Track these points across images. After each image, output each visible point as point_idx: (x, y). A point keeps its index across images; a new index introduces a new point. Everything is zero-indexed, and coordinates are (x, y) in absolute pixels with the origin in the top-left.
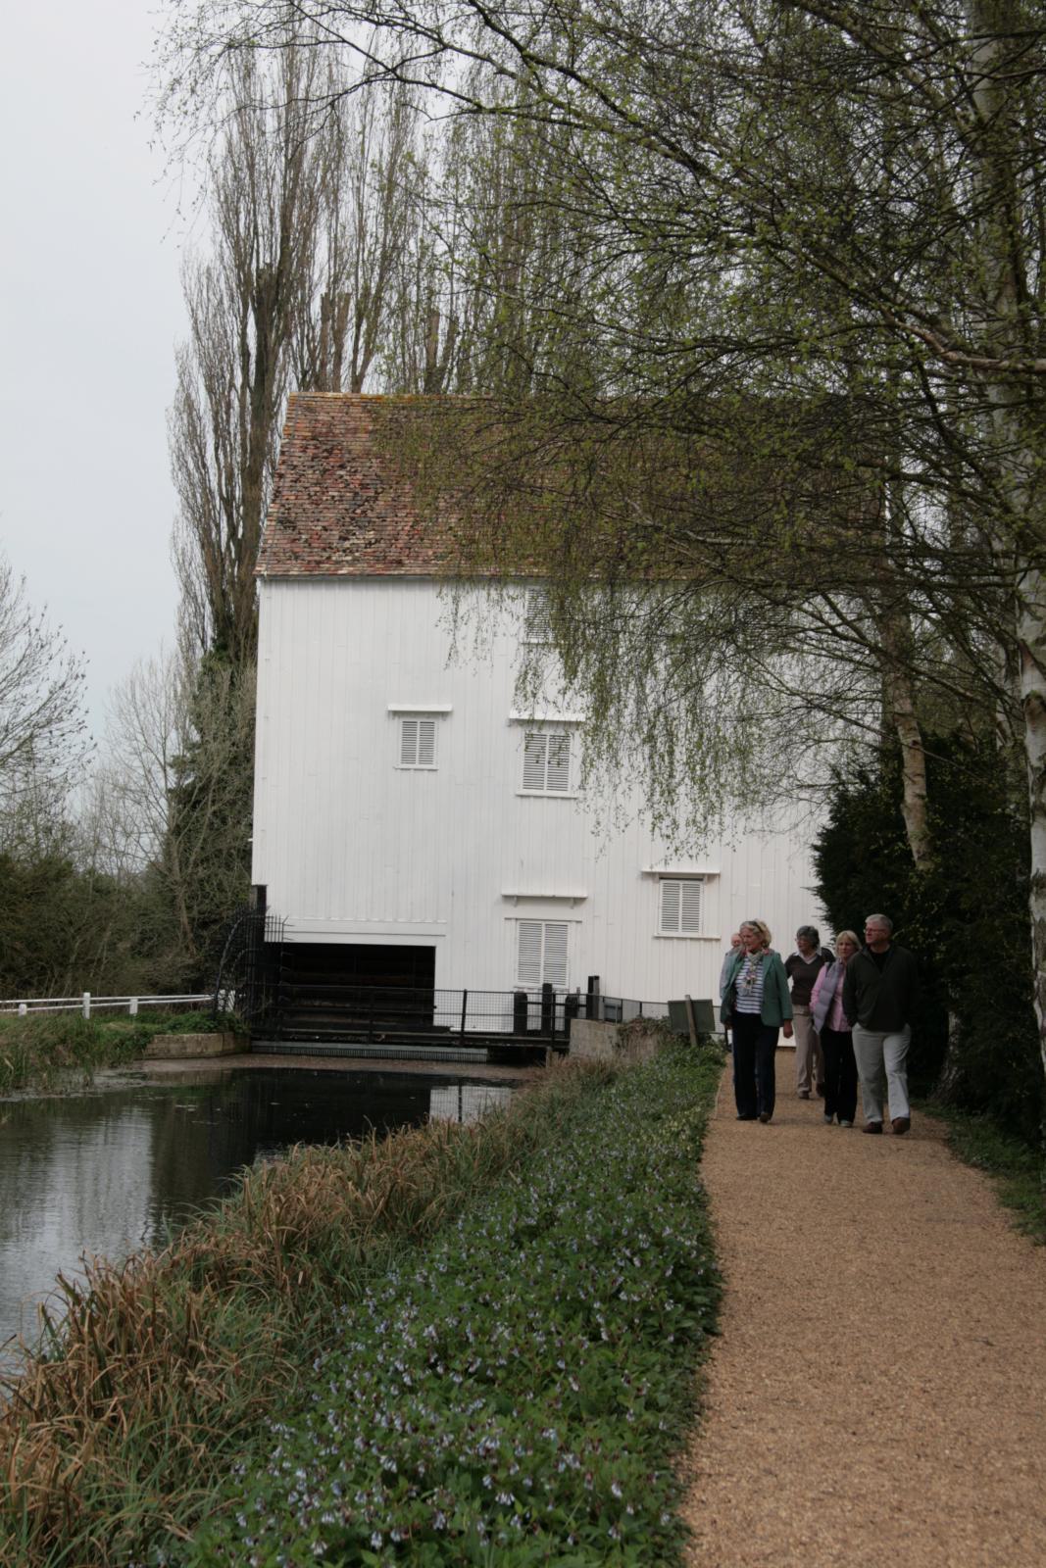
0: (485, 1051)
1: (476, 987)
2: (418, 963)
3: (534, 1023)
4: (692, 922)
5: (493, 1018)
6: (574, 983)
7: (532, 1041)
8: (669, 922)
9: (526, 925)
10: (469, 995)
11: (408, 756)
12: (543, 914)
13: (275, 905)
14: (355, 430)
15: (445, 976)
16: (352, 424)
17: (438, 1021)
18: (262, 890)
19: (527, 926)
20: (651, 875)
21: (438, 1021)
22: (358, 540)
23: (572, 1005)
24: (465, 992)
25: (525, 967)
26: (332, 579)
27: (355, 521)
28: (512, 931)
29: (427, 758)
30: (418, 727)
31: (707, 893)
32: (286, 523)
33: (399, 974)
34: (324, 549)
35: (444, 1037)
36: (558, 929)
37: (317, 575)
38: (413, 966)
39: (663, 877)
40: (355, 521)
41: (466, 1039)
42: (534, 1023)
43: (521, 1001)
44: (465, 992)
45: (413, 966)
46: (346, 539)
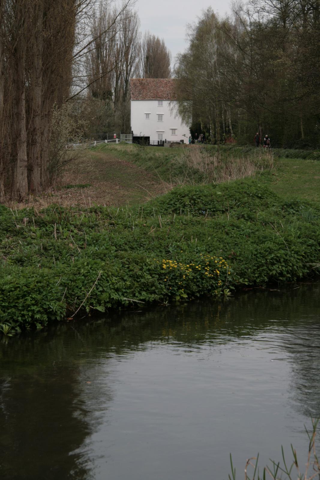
1: (154, 140)
3: (160, 144)
4: (175, 133)
6: (164, 139)
7: (161, 144)
8: (172, 133)
9: (159, 134)
12: (160, 133)
13: (134, 133)
15: (151, 139)
19: (159, 134)
22: (140, 96)
23: (163, 142)
25: (159, 138)
26: (138, 100)
27: (140, 94)
28: (157, 135)
29: (148, 118)
30: (148, 115)
31: (176, 131)
32: (133, 94)
33: (147, 139)
36: (162, 135)
37: (137, 100)
38: (147, 138)
40: (140, 94)
42: (160, 144)
43: (158, 142)
45: (147, 138)
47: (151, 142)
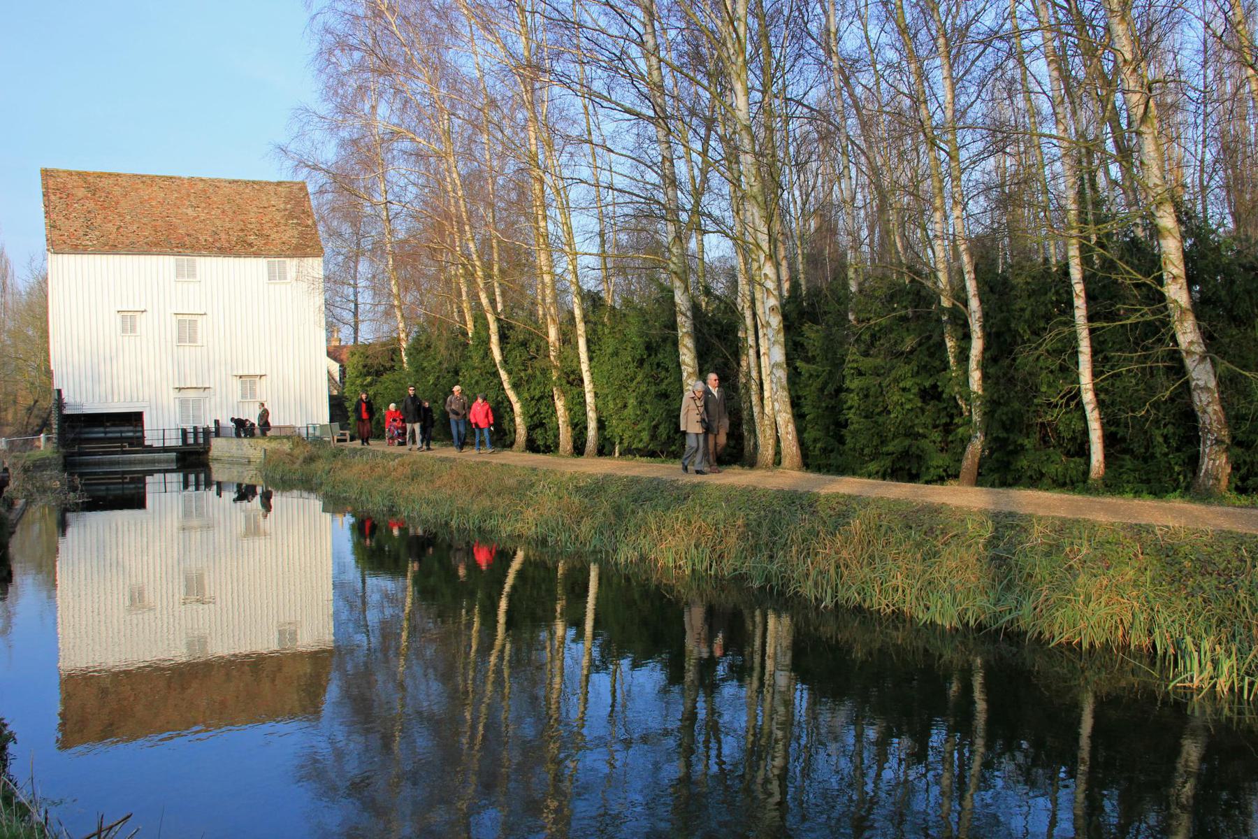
3: (191, 441)
5: (174, 440)
11: (124, 330)
18: (59, 391)
29: (133, 329)
35: (151, 449)
41: (165, 450)
42: (191, 441)
43: (184, 432)
45: (134, 419)
47: (151, 438)
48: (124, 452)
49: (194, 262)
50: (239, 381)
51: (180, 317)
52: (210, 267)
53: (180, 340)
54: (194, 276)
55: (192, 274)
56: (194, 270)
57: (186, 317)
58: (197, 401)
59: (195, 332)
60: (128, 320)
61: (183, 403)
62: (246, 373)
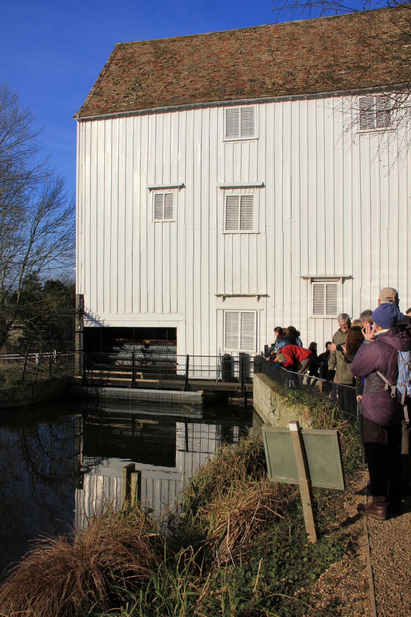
0: (200, 393)
2: (168, 335)
10: (191, 358)
11: (157, 214)
13: (88, 306)
14: (145, 54)
15: (182, 347)
16: (144, 52)
17: (179, 373)
18: (82, 297)
20: (307, 278)
21: (179, 373)
24: (188, 357)
29: (169, 212)
34: (114, 103)
39: (312, 280)
44: (188, 357)
46: (126, 97)
48: (135, 385)
49: (252, 111)
50: (311, 287)
51: (229, 192)
52: (272, 116)
53: (228, 226)
54: (251, 131)
55: (248, 129)
56: (252, 124)
57: (237, 192)
58: (247, 315)
59: (250, 214)
60: (163, 200)
61: (228, 315)
62: (321, 274)
